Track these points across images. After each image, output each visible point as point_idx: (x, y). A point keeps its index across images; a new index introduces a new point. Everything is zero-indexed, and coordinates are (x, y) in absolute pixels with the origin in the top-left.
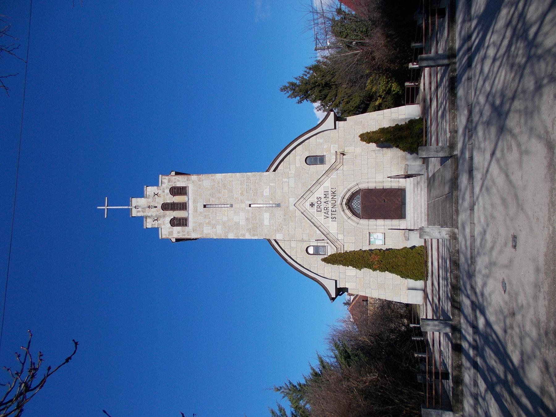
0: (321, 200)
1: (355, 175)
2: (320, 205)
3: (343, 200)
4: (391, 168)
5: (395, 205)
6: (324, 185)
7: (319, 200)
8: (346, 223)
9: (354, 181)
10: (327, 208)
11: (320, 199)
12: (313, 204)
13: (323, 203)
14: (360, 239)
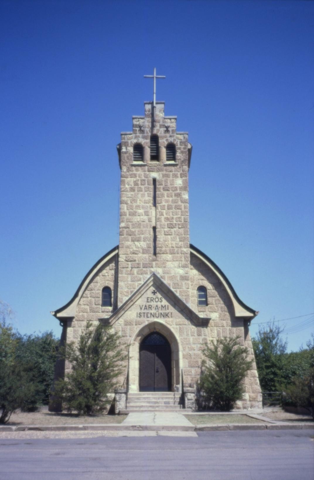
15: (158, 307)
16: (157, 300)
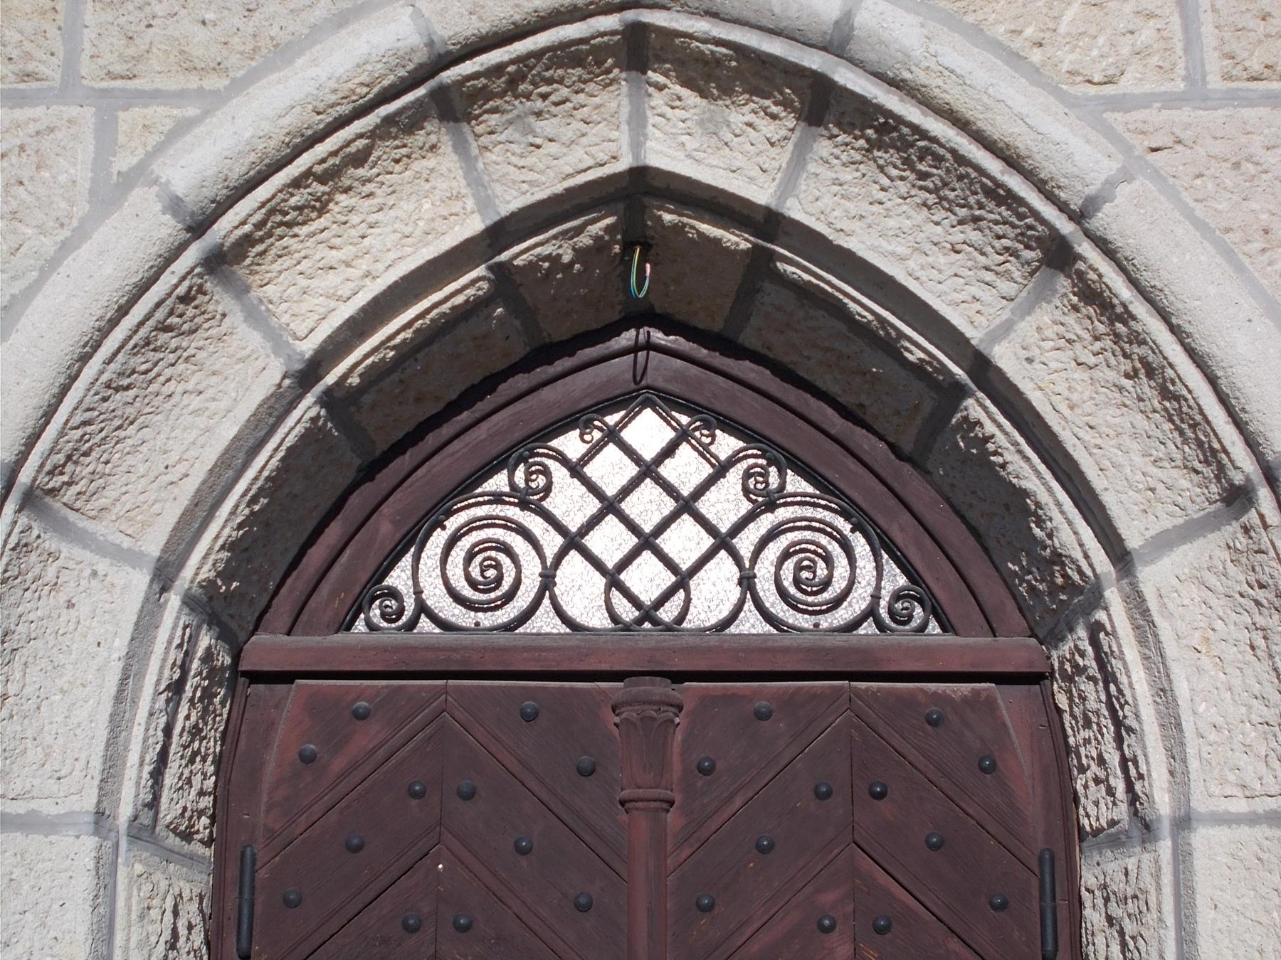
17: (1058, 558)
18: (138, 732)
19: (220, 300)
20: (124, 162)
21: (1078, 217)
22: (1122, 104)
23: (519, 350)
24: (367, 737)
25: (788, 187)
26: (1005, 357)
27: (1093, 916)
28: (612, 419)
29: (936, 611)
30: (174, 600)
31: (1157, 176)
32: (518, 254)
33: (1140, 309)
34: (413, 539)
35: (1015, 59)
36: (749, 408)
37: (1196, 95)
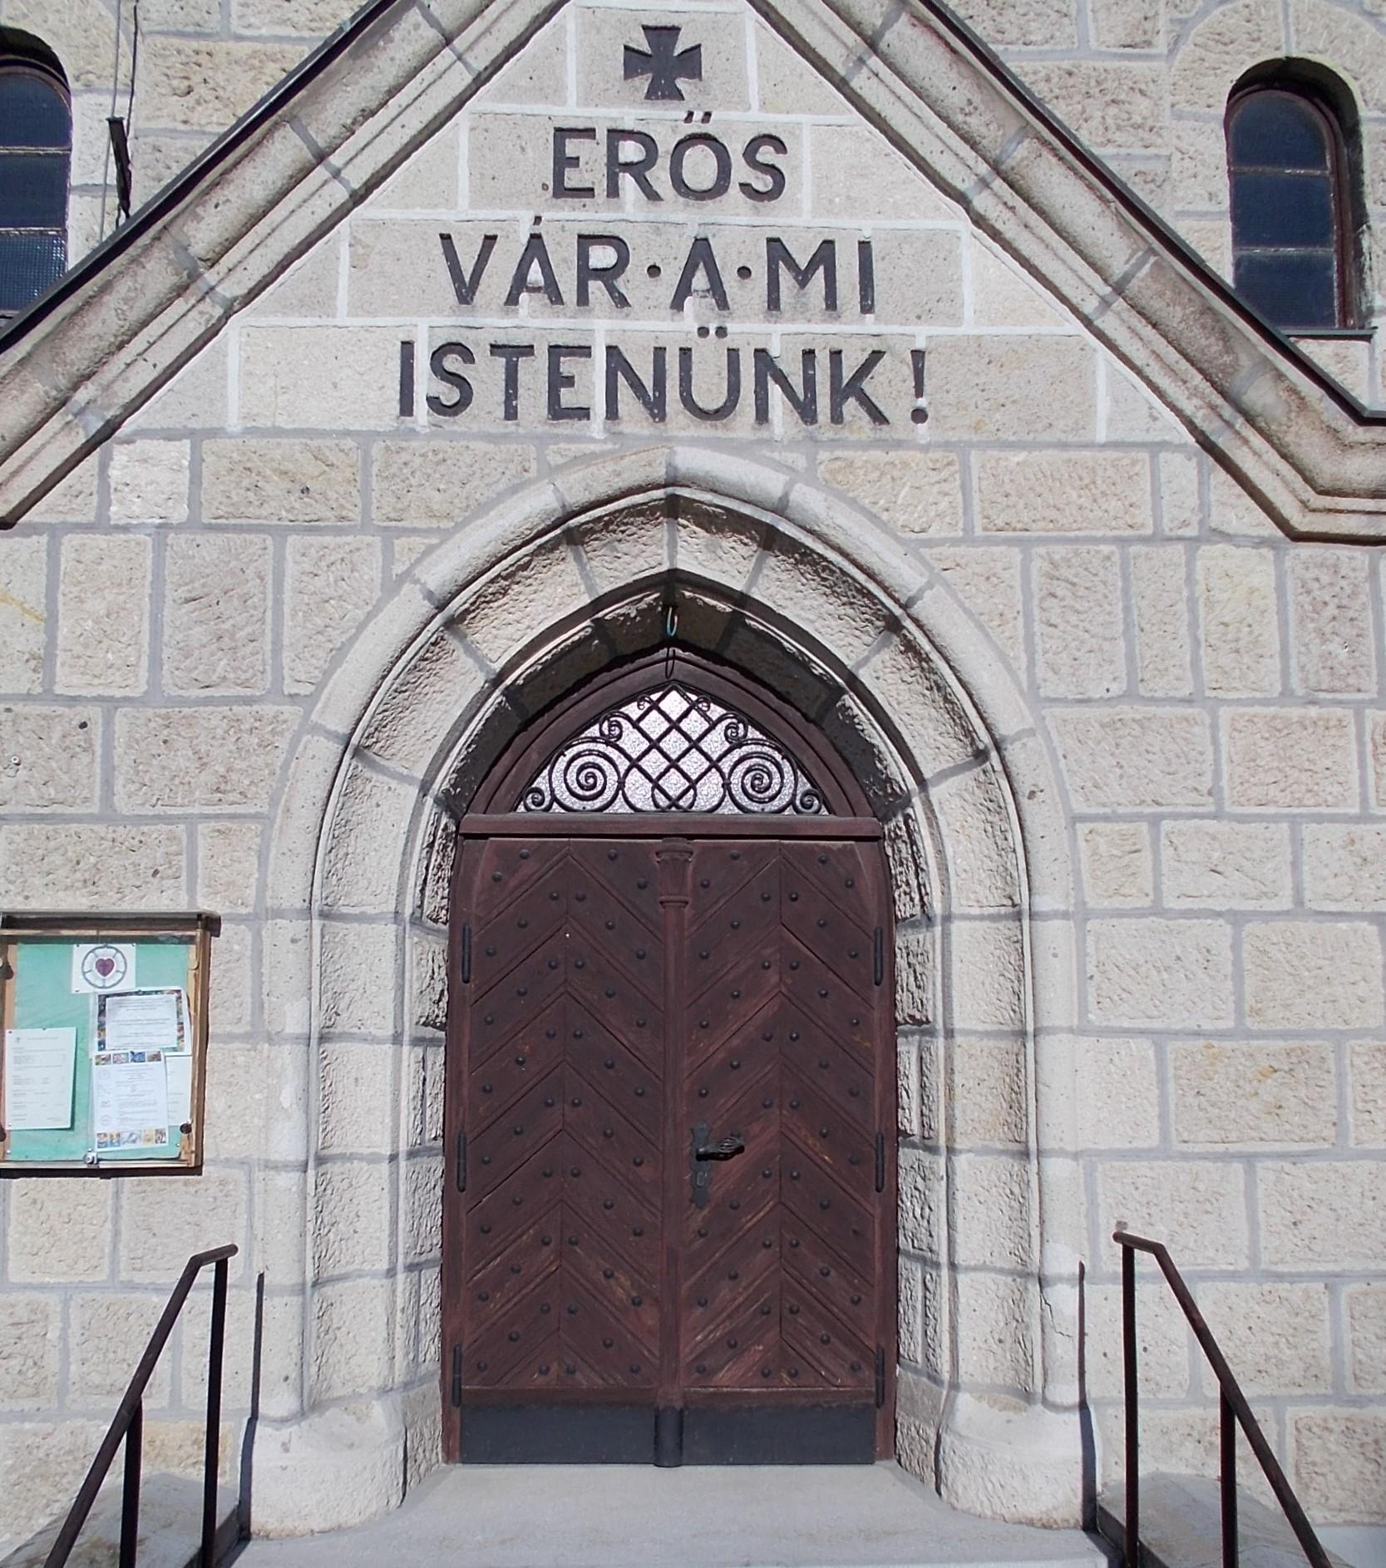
0: (734, 190)
1: (1126, 711)
2: (660, 176)
3: (728, 542)
4: (1233, 1276)
5: (650, 1317)
6: (972, 247)
7: (741, 172)
8: (372, 571)
9: (1034, 696)
10: (607, 275)
11: (745, 187)
12: (682, 84)
13: (689, 219)
14: (108, 784)
15: (730, 280)
16: (700, 167)
17: (889, 780)
18: (413, 870)
19: (452, 643)
20: (399, 569)
21: (904, 607)
22: (929, 543)
23: (605, 661)
24: (528, 868)
25: (752, 581)
26: (865, 676)
27: (901, 962)
28: (655, 697)
29: (825, 802)
30: (429, 800)
31: (947, 585)
32: (608, 613)
33: (934, 656)
34: (549, 761)
35: (873, 518)
36: (729, 692)
37: (968, 539)
